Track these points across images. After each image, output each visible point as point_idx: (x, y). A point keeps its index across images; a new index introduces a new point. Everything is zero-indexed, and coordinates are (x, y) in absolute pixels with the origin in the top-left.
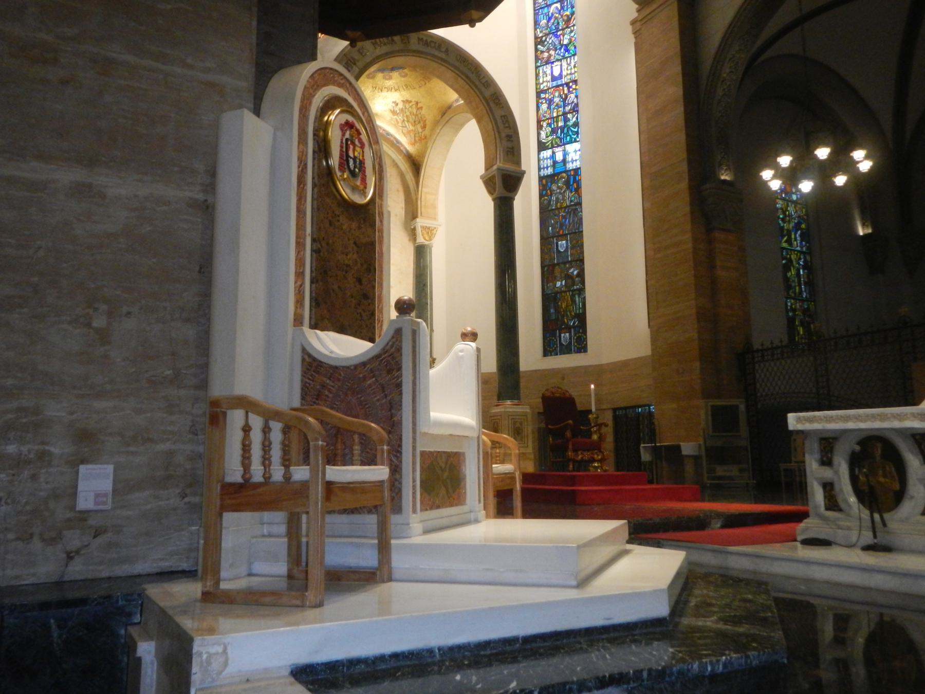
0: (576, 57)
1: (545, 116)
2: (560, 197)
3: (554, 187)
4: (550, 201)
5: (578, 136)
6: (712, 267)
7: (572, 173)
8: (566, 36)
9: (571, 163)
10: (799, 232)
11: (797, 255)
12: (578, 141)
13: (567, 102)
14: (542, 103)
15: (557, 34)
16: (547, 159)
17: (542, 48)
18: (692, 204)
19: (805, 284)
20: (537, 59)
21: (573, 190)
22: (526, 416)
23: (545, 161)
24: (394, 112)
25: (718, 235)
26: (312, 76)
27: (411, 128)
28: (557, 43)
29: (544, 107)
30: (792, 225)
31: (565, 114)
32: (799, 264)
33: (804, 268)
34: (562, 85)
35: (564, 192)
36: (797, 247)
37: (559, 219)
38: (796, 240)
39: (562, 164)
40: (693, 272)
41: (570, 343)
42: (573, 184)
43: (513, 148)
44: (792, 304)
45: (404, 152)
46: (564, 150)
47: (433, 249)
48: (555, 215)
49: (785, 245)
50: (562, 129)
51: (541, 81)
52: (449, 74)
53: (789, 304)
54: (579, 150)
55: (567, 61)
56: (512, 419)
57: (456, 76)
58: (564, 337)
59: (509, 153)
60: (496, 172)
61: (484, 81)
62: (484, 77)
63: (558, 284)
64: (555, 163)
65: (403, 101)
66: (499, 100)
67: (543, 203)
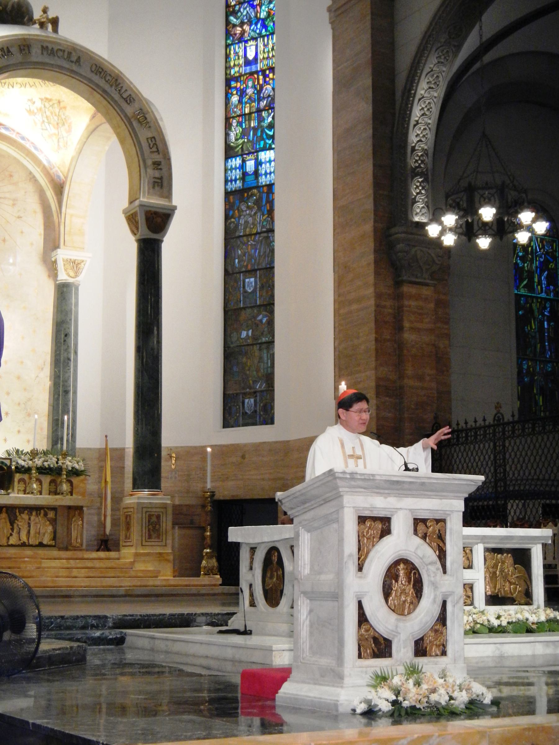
0: (275, 36)
1: (235, 112)
2: (250, 220)
3: (243, 207)
4: (237, 226)
5: (273, 142)
6: (400, 329)
7: (265, 189)
8: (263, 7)
9: (264, 177)
10: (546, 273)
11: (540, 303)
12: (273, 149)
13: (262, 95)
14: (232, 94)
15: (253, 4)
16: (236, 168)
17: (235, 20)
18: (376, 251)
20: (228, 34)
21: (266, 212)
22: (166, 508)
23: (234, 171)
24: (30, 112)
25: (406, 289)
27: (54, 131)
29: (235, 99)
30: (536, 264)
31: (259, 111)
32: (544, 315)
34: (257, 72)
35: (255, 214)
36: (542, 292)
37: (248, 249)
38: (540, 283)
39: (253, 177)
40: (374, 335)
41: (255, 411)
42: (266, 204)
43: (161, 178)
44: (529, 367)
45: (45, 162)
46: (256, 159)
47: (80, 288)
48: (244, 244)
49: (523, 292)
50: (255, 129)
51: (232, 64)
52: (83, 87)
53: (525, 367)
54: (274, 161)
55: (264, 40)
56: (146, 512)
57: (90, 89)
58: (248, 403)
59: (156, 184)
60: (138, 209)
61: (125, 96)
62: (126, 90)
63: (244, 334)
64: (245, 174)
65: (42, 100)
66: (146, 118)
67: (230, 227)
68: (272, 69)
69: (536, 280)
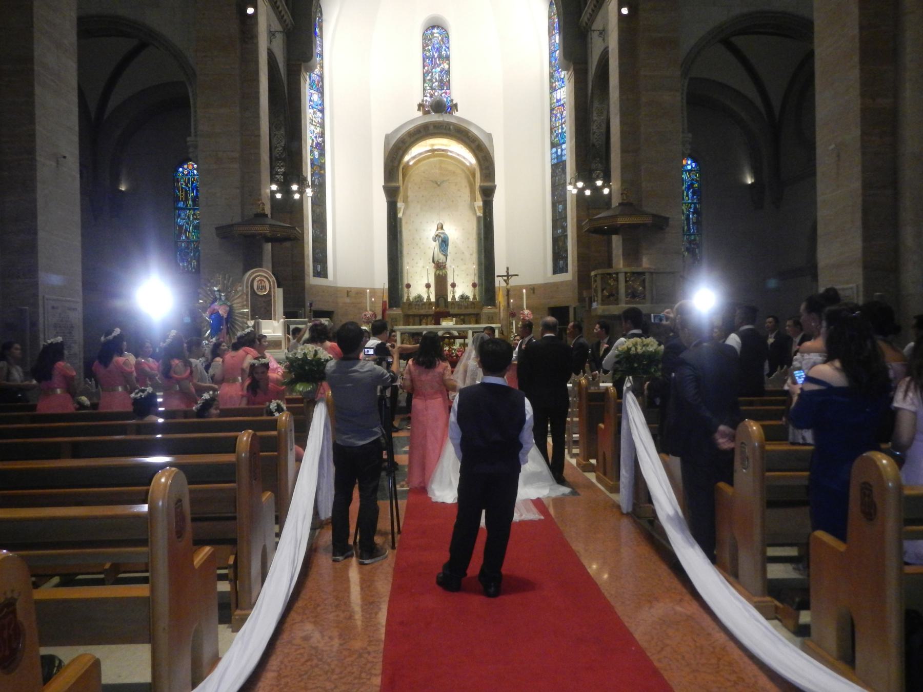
3: (557, 172)
4: (555, 181)
10: (691, 190)
11: (688, 206)
19: (694, 223)
20: (551, 87)
26: (250, 275)
28: (559, 77)
29: (554, 119)
31: (562, 124)
32: (689, 211)
33: (693, 213)
34: (560, 106)
38: (687, 195)
41: (563, 267)
45: (468, 164)
50: (561, 134)
61: (471, 140)
64: (557, 156)
68: (565, 103)
69: (685, 194)
